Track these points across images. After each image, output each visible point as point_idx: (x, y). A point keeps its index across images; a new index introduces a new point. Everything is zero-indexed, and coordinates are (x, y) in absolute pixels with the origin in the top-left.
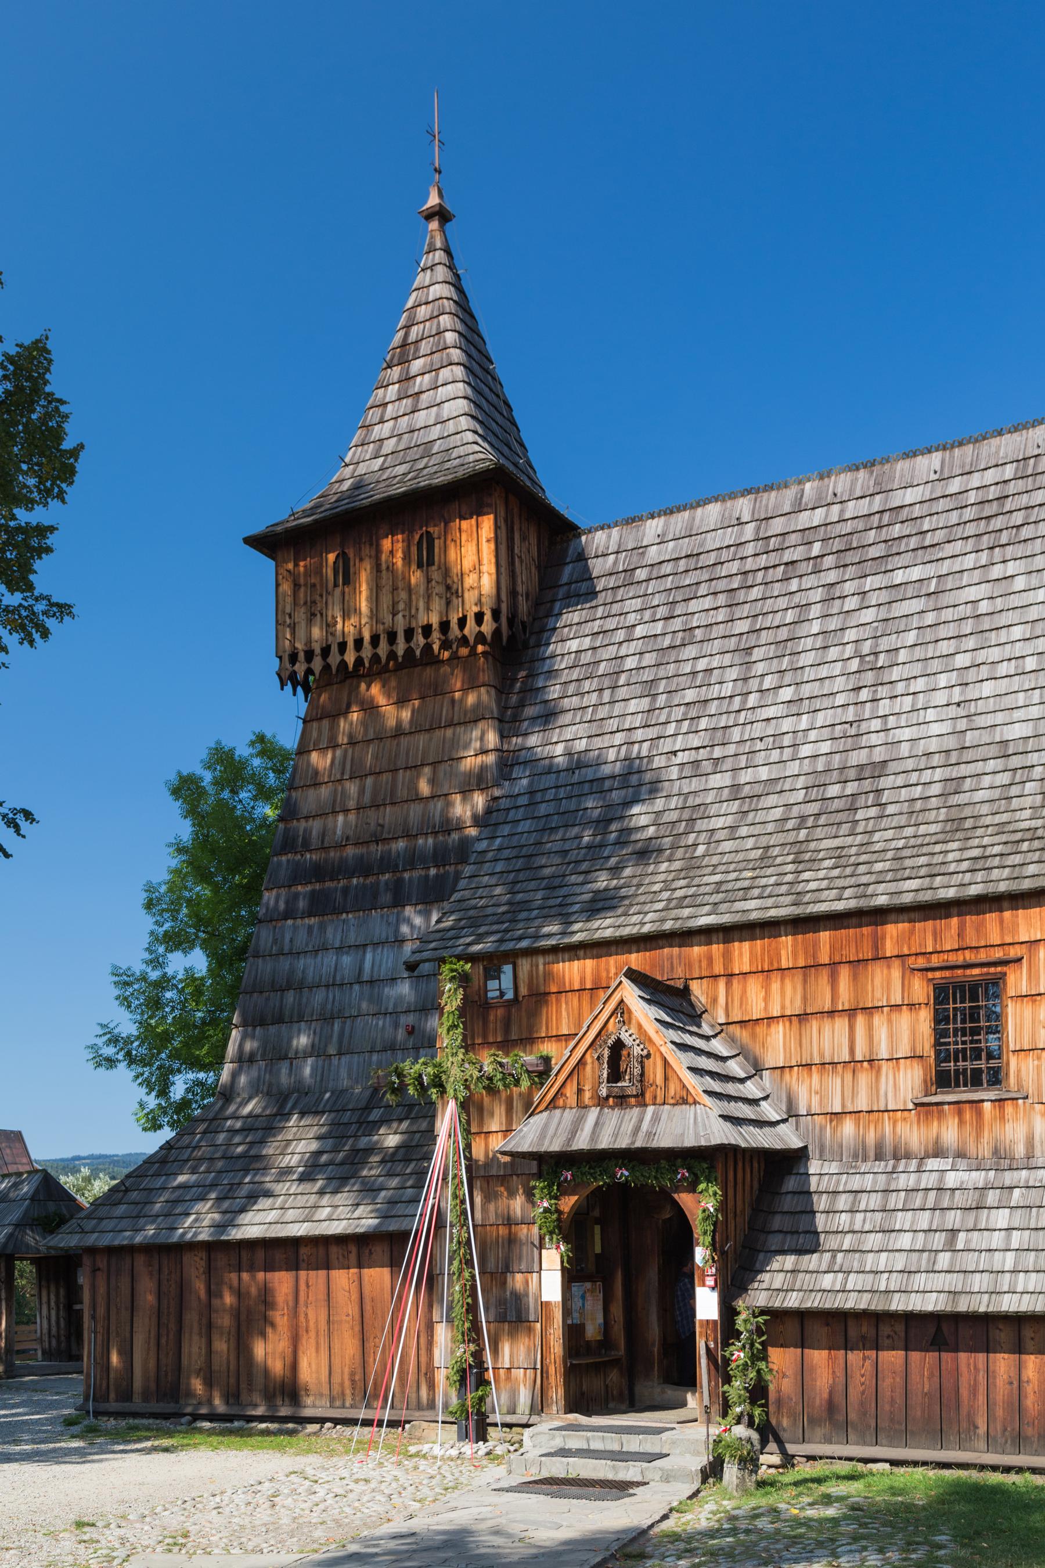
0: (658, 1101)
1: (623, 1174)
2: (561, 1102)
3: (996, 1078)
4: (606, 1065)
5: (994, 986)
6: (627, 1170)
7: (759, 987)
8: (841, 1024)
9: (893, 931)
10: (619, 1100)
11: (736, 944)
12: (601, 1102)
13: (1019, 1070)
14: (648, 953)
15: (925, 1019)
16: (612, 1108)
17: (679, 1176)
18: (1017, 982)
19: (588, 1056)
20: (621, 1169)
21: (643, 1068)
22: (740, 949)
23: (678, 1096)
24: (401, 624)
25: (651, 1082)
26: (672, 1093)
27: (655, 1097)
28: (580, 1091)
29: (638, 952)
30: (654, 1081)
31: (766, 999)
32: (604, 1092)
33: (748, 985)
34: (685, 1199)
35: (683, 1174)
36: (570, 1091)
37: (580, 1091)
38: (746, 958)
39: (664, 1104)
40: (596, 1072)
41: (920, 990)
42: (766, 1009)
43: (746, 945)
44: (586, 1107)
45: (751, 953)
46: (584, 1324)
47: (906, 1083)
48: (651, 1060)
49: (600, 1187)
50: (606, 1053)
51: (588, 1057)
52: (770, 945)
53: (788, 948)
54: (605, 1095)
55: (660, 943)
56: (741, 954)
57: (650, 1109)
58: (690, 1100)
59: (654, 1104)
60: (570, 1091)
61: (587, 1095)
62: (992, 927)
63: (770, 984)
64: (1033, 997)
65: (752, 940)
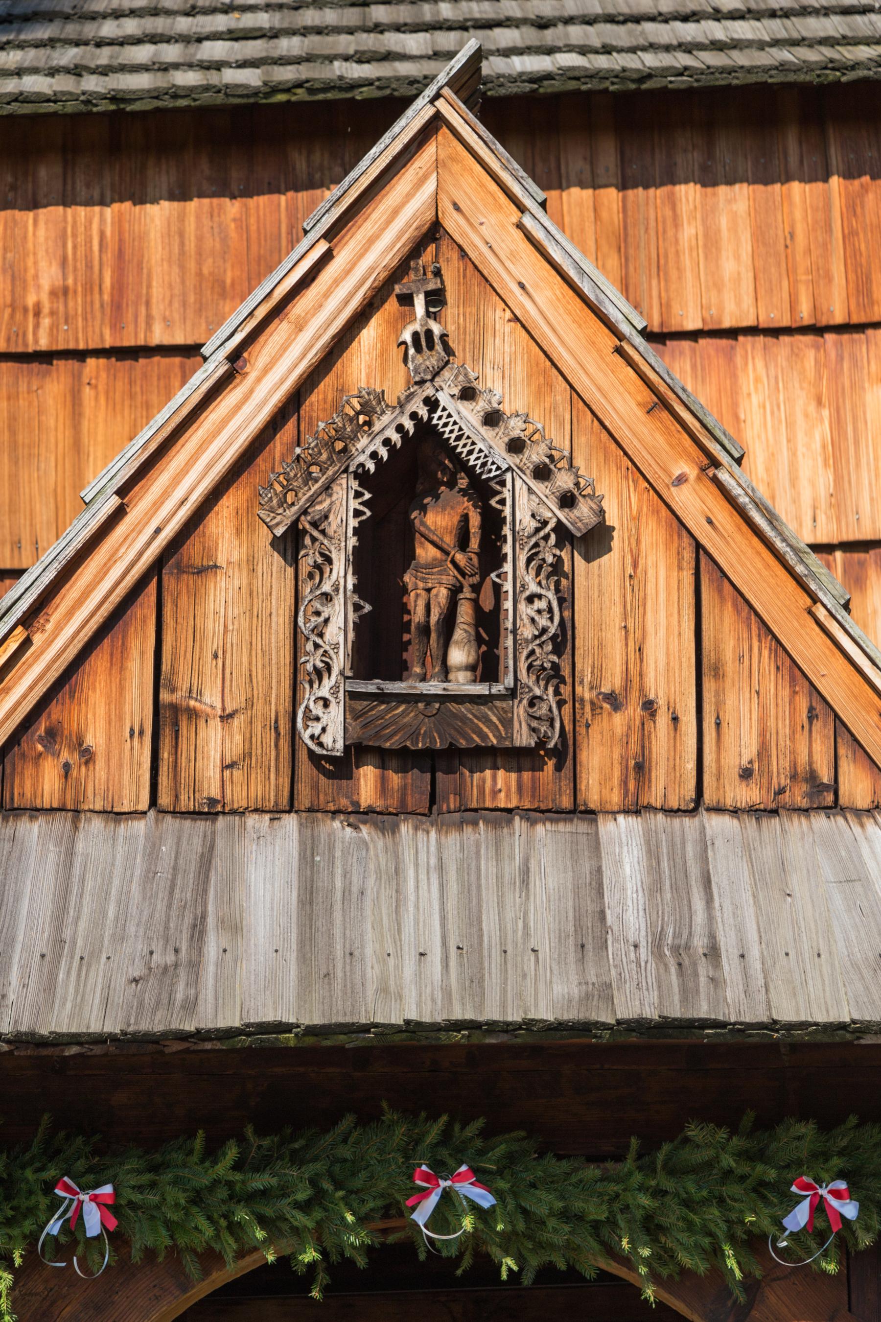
0: (655, 796)
1: (454, 1203)
2: (46, 781)
4: (341, 573)
6: (482, 1177)
7: (802, 401)
10: (418, 779)
11: (688, 193)
12: (315, 782)
14: (232, 208)
16: (383, 818)
17: (799, 1217)
19: (221, 524)
20: (441, 1169)
21: (566, 600)
22: (708, 214)
23: (779, 767)
25: (613, 681)
26: (740, 744)
27: (641, 769)
28: (168, 720)
29: (181, 194)
30: (633, 677)
31: (838, 455)
32: (332, 728)
33: (747, 382)
35: (819, 1207)
36: (111, 714)
37: (168, 720)
38: (736, 261)
39: (697, 804)
40: (255, 627)
42: (838, 499)
43: (737, 201)
44: (210, 811)
45: (760, 236)
48: (611, 563)
49: (282, 1279)
50: (344, 509)
51: (224, 535)
52: (852, 207)
54: (334, 740)
55: (300, 162)
56: (711, 242)
57: (624, 840)
58: (857, 786)
59: (636, 809)
60: (111, 714)
61: (212, 747)
63: (857, 387)
65: (766, 180)
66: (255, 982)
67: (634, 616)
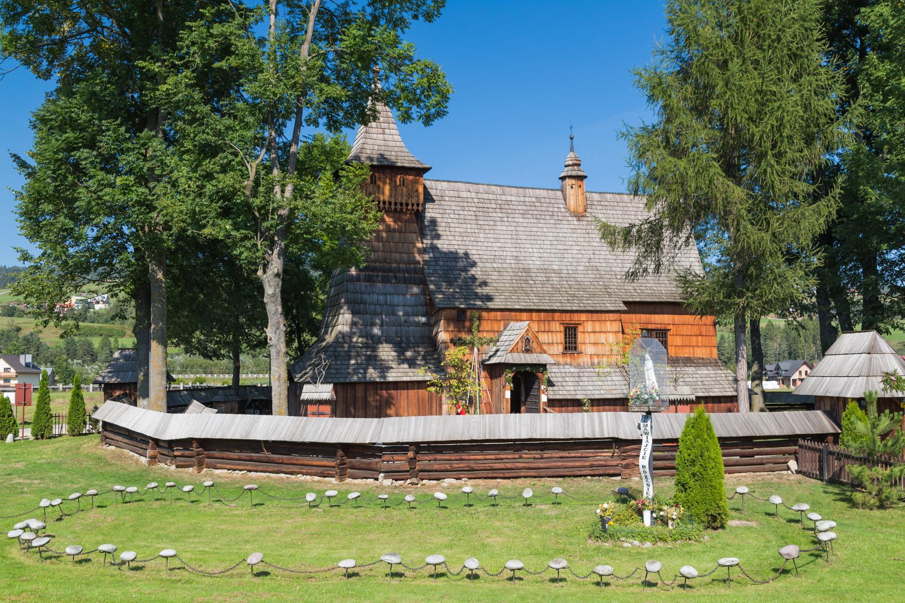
1: (528, 369)
3: (575, 349)
5: (575, 329)
8: (546, 334)
9: (557, 314)
13: (581, 348)
15: (563, 334)
18: (580, 329)
24: (393, 201)
34: (539, 375)
41: (562, 329)
46: (270, 412)
47: (560, 348)
53: (534, 314)
62: (576, 317)
64: (584, 332)
66: (523, 361)
67: (534, 345)
